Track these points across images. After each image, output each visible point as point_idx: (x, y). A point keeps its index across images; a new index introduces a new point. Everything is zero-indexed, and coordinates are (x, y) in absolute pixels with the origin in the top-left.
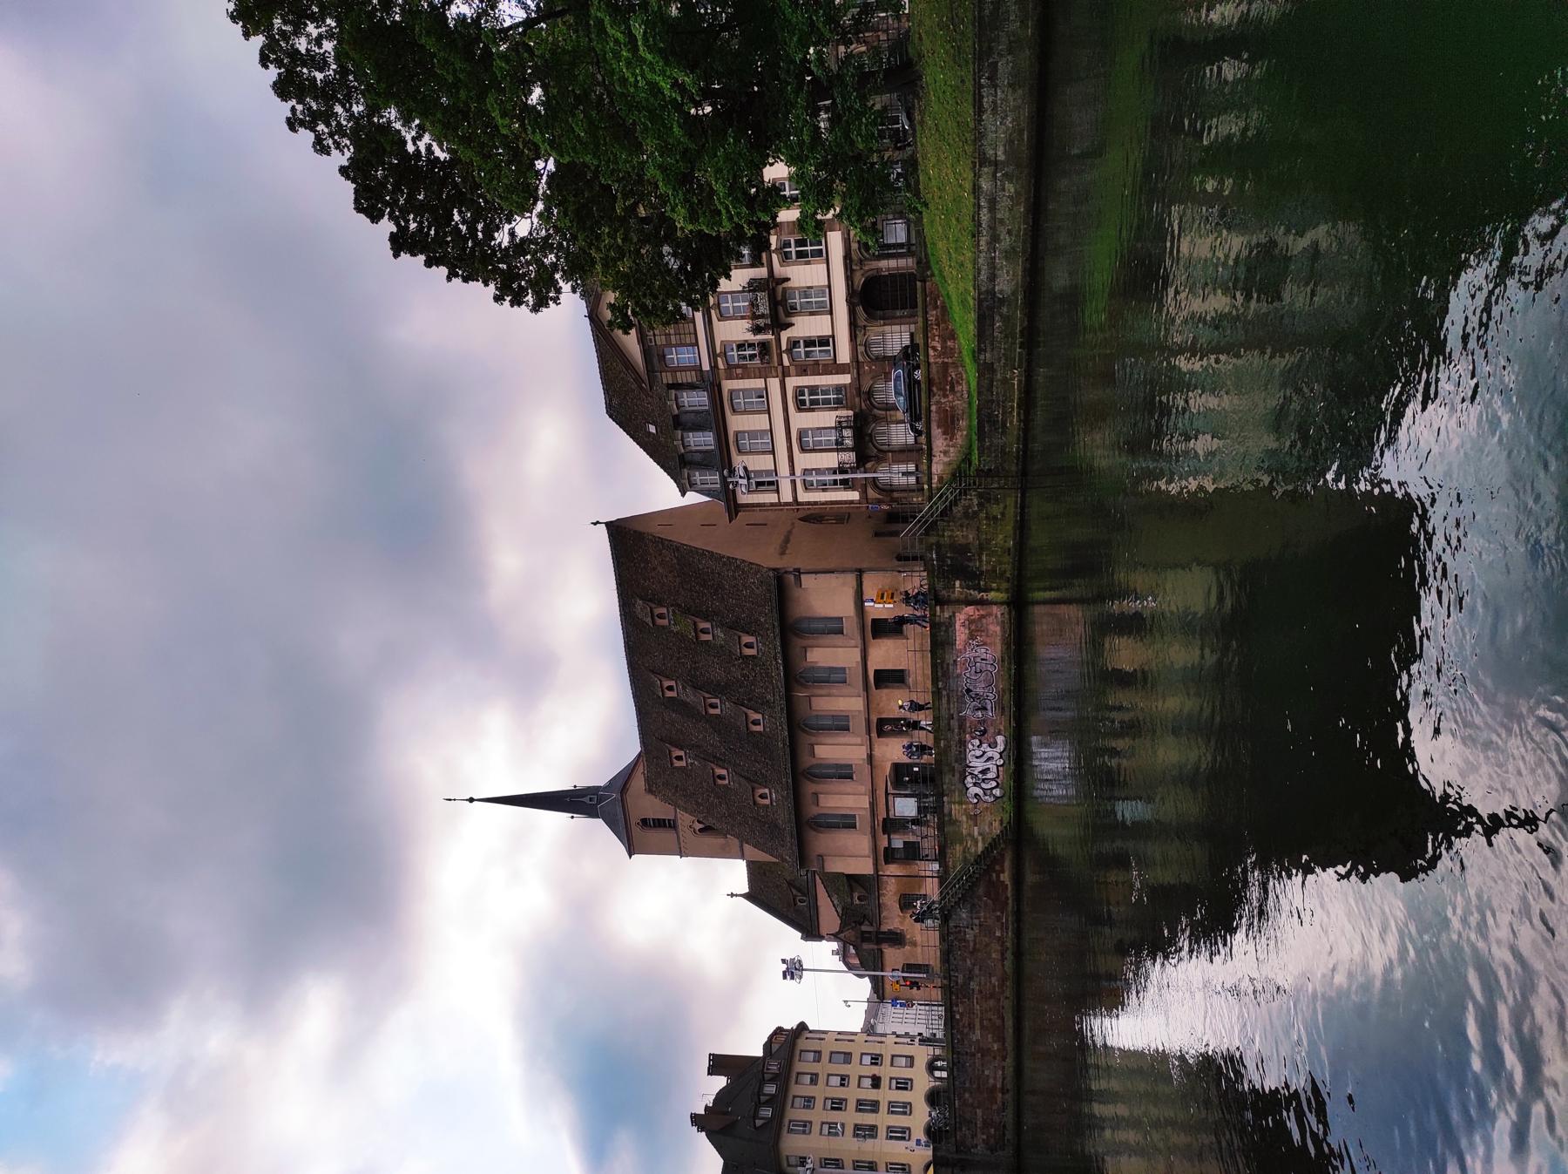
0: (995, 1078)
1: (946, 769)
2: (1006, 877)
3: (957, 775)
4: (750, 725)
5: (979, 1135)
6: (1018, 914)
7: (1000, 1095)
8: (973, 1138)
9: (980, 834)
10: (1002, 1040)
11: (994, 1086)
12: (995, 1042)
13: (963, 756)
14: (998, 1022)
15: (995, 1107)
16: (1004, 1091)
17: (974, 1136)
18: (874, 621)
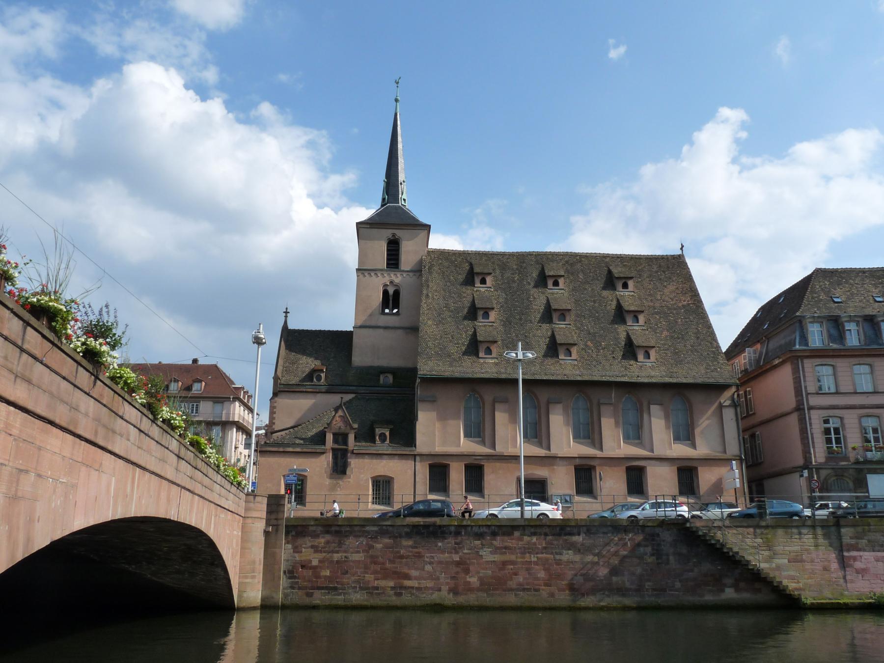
0: (416, 578)
1: (860, 529)
2: (729, 594)
3: (853, 541)
4: (565, 347)
5: (316, 555)
6: (680, 608)
7: (391, 584)
8: (312, 547)
9: (778, 568)
10: (486, 586)
11: (407, 577)
12: (481, 579)
13: (877, 548)
14: (512, 584)
15: (369, 577)
16: (399, 590)
17: (316, 550)
18: (696, 468)
